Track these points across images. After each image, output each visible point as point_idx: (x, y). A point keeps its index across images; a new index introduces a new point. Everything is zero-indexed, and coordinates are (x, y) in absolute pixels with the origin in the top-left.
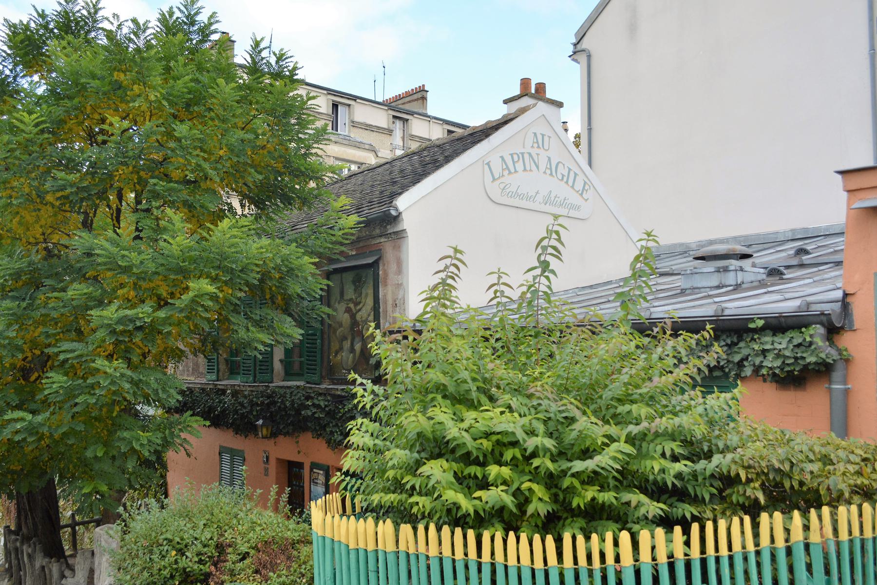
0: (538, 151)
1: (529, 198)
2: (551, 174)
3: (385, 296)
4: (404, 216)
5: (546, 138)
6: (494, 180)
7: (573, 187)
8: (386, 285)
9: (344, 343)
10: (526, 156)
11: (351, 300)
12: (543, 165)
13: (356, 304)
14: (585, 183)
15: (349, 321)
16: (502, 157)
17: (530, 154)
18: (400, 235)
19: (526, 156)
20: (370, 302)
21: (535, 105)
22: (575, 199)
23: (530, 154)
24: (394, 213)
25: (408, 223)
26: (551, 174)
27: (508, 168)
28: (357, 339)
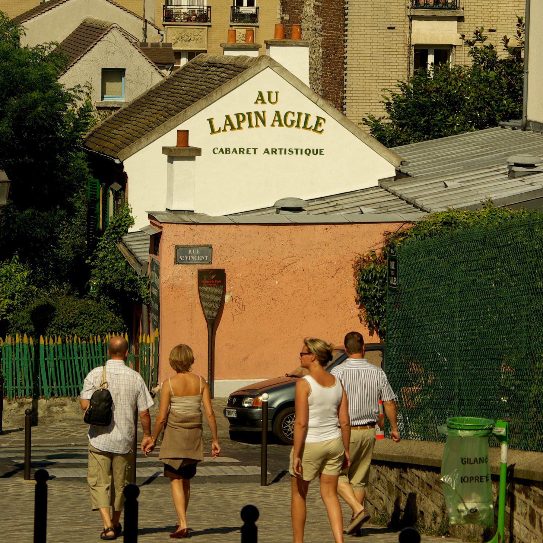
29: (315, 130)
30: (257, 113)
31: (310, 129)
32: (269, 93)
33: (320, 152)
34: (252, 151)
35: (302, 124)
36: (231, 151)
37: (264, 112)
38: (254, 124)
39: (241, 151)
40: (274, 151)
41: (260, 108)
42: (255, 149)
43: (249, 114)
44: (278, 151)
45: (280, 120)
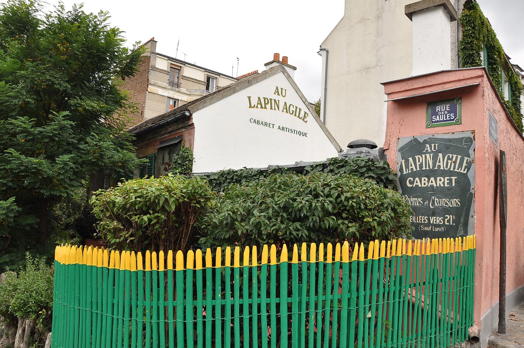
24: (187, 114)
29: (303, 120)
30: (275, 100)
31: (301, 118)
32: (282, 89)
33: (305, 135)
34: (271, 126)
35: (297, 115)
36: (260, 123)
37: (278, 101)
38: (273, 108)
39: (266, 124)
40: (283, 129)
41: (276, 97)
42: (273, 125)
43: (271, 99)
44: (285, 129)
45: (287, 109)
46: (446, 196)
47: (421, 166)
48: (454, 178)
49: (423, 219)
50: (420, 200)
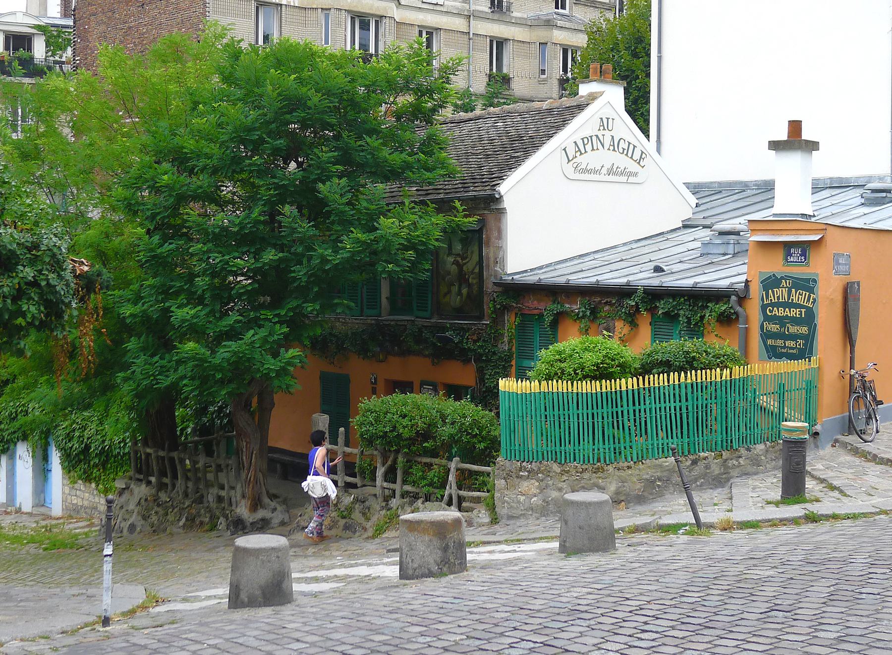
0: (603, 132)
1: (596, 172)
2: (614, 150)
3: (488, 254)
4: (504, 198)
5: (610, 121)
6: (569, 161)
7: (631, 158)
8: (488, 245)
9: (452, 288)
10: (594, 138)
11: (458, 255)
12: (607, 142)
13: (463, 258)
14: (642, 152)
15: (457, 271)
16: (575, 142)
17: (597, 136)
18: (502, 212)
19: (594, 138)
20: (476, 258)
21: (602, 93)
22: (633, 167)
23: (597, 136)
24: (497, 196)
25: (507, 203)
26: (614, 150)
27: (579, 150)
28: (464, 286)
46: (798, 324)
47: (778, 298)
48: (803, 310)
49: (780, 342)
50: (778, 326)
